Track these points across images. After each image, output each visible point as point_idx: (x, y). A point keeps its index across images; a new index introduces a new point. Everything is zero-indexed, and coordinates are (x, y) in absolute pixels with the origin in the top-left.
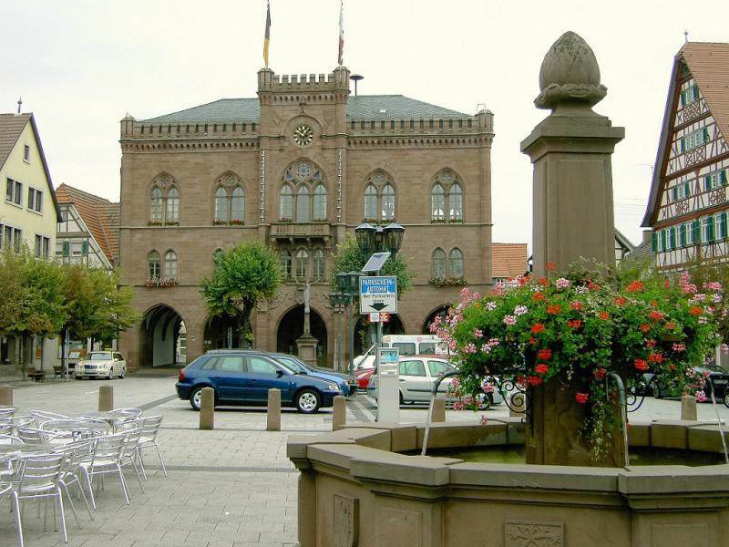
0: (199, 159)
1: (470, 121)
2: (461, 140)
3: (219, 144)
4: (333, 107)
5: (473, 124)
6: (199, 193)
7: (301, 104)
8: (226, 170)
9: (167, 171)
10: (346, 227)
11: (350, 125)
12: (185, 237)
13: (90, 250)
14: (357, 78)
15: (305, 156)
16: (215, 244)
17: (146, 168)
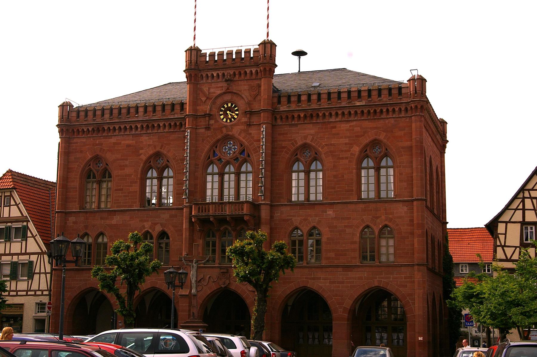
0: (130, 141)
1: (400, 89)
2: (391, 109)
3: (149, 126)
4: (258, 82)
5: (403, 91)
7: (226, 81)
8: (155, 151)
10: (271, 206)
11: (276, 100)
12: (116, 220)
13: (29, 234)
15: (230, 133)
17: (81, 152)
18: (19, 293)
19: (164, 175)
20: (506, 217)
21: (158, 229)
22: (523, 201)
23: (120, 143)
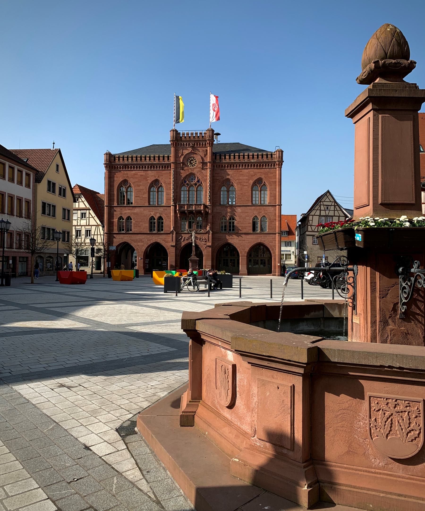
0: (142, 173)
3: (152, 166)
4: (206, 148)
6: (143, 190)
8: (155, 179)
9: (127, 179)
12: (137, 210)
14: (218, 134)
15: (193, 172)
16: (151, 214)
18: (86, 244)
19: (151, 190)
20: (312, 213)
21: (158, 215)
22: (320, 207)
23: (137, 174)
